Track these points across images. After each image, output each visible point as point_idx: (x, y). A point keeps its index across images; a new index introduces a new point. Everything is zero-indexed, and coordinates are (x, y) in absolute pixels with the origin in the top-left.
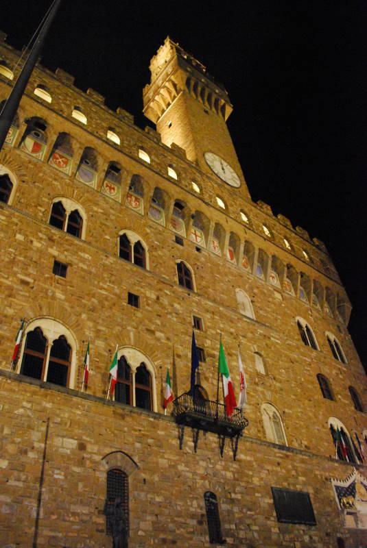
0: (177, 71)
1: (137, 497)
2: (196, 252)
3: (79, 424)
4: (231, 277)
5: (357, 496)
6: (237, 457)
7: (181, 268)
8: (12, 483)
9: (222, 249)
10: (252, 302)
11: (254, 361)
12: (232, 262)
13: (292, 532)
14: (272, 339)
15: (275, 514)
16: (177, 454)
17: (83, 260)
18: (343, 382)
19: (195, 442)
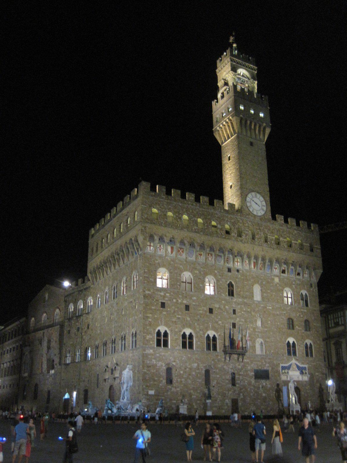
0: (234, 116)
1: (212, 376)
2: (237, 273)
3: (197, 359)
4: (252, 280)
5: (291, 369)
6: (244, 361)
7: (230, 285)
8: (184, 376)
9: (250, 264)
10: (261, 290)
11: (256, 321)
12: (254, 270)
13: (259, 382)
14: (268, 307)
15: (254, 377)
16: (224, 363)
17: (194, 301)
18: (302, 319)
19: (230, 358)
